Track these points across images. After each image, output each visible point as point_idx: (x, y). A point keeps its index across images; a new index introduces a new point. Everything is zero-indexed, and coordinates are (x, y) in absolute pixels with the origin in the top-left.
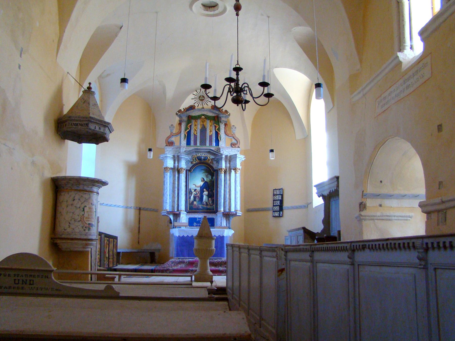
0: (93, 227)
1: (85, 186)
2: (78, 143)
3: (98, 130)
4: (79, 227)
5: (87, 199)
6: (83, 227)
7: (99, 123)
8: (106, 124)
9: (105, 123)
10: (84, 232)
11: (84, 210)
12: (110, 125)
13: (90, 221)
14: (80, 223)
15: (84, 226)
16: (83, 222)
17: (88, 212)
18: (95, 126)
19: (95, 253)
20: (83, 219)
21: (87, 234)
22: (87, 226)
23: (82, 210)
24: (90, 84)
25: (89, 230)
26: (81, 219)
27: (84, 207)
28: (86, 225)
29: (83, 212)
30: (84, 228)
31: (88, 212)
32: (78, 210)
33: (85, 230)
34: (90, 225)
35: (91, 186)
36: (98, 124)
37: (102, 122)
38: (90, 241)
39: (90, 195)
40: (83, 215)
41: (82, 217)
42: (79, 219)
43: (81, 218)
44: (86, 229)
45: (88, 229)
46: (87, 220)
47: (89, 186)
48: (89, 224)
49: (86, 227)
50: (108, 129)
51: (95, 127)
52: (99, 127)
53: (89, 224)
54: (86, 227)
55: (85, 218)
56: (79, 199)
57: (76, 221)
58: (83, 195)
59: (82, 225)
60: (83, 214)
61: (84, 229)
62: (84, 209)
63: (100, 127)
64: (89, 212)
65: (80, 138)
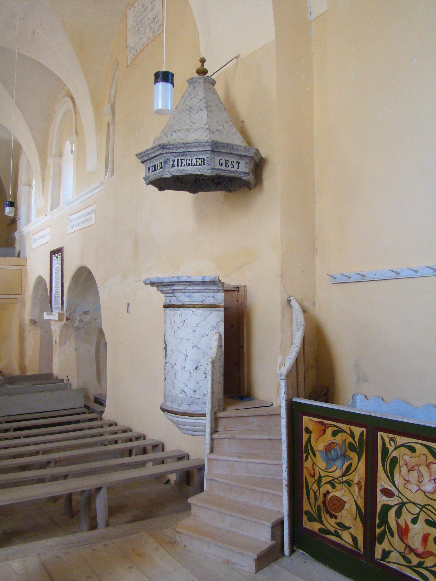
24: (203, 61)
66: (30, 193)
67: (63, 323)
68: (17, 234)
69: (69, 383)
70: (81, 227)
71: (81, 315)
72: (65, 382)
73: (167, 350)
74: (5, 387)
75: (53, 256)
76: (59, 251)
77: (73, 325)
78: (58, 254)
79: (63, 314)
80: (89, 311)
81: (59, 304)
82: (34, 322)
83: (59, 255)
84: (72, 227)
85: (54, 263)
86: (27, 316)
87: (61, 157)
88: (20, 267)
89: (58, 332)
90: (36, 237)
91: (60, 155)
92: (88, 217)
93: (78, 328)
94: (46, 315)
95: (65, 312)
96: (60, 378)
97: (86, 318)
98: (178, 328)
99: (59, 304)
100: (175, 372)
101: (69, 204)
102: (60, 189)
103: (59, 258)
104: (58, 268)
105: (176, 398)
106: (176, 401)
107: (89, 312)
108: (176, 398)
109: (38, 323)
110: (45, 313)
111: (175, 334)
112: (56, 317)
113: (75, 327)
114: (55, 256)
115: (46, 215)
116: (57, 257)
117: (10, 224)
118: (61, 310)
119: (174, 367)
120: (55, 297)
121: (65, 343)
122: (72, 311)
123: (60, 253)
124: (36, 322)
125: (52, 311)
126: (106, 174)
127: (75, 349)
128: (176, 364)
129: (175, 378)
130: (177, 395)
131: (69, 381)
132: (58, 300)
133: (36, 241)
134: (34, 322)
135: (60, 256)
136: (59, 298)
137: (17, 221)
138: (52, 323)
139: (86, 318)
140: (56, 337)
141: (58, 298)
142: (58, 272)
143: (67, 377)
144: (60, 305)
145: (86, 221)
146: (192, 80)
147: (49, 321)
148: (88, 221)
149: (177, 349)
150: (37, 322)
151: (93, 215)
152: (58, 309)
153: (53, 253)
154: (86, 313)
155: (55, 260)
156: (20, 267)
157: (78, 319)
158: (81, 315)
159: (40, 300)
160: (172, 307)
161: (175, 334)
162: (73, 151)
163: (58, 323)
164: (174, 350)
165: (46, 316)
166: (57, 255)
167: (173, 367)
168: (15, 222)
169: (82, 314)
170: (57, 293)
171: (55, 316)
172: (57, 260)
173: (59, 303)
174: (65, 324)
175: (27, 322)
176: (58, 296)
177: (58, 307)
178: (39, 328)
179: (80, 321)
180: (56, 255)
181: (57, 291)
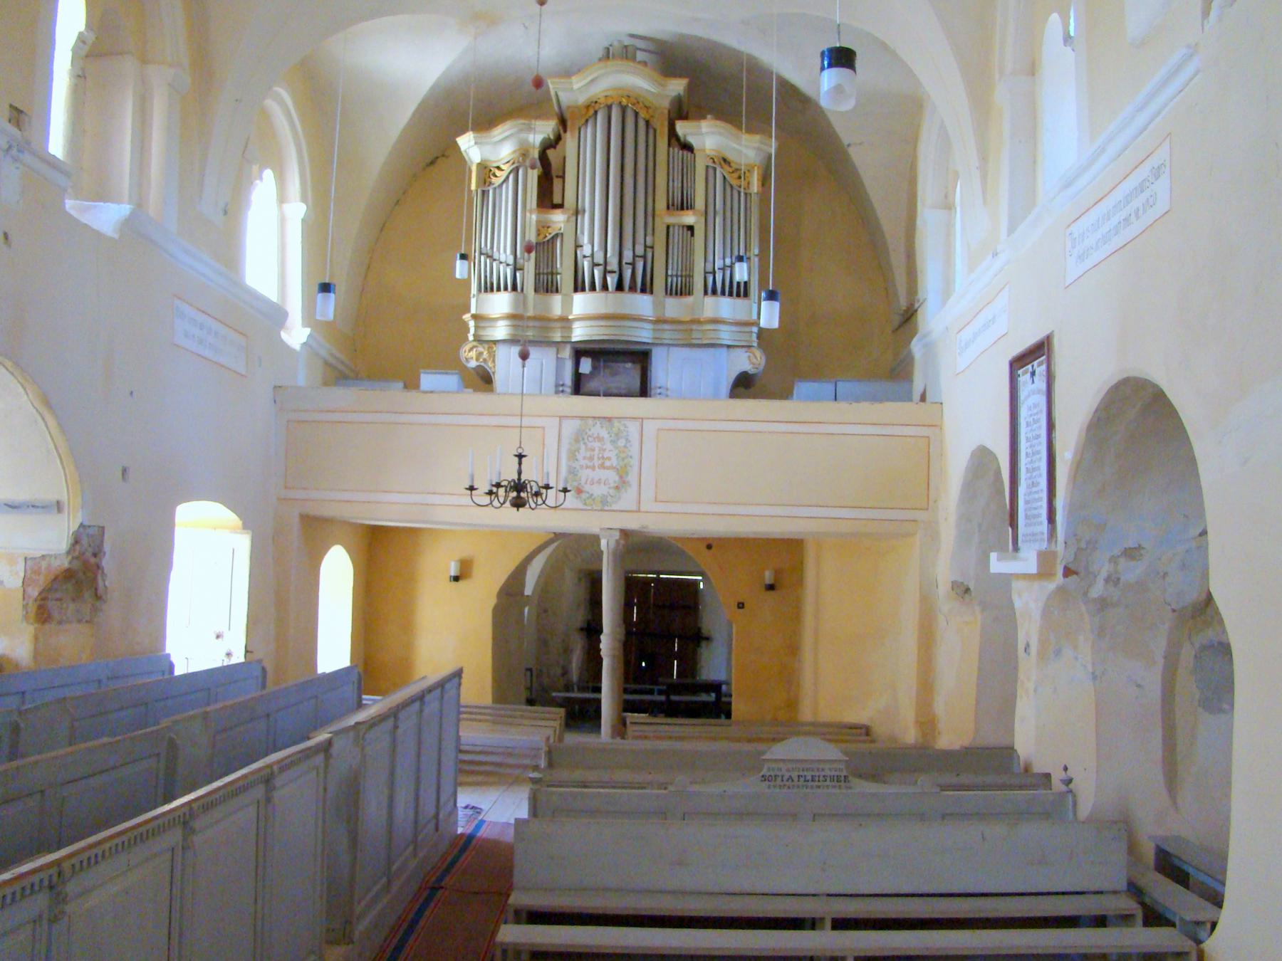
66: (949, 226)
67: (1051, 586)
68: (916, 347)
69: (1071, 791)
70: (1117, 241)
71: (1113, 560)
72: (1057, 786)
74: (850, 788)
75: (1020, 372)
76: (1040, 350)
77: (1085, 594)
78: (1035, 363)
79: (1054, 554)
80: (1140, 548)
81: (1041, 523)
82: (962, 590)
83: (1040, 365)
84: (1081, 258)
85: (1023, 394)
86: (944, 572)
87: (1033, 75)
88: (925, 431)
89: (1036, 615)
90: (967, 334)
91: (1032, 69)
92: (1137, 202)
93: (1103, 604)
94: (999, 559)
95: (1060, 547)
96: (1038, 768)
97: (1132, 572)
99: (1041, 523)
101: (1068, 185)
102: (1034, 170)
103: (1040, 376)
104: (1035, 406)
107: (1142, 552)
109: (973, 594)
110: (993, 556)
112: (1033, 569)
113: (1094, 600)
114: (1025, 373)
115: (995, 254)
116: (1033, 374)
117: (900, 326)
118: (1046, 543)
120: (1027, 502)
121: (1058, 652)
122: (1083, 545)
123: (1044, 357)
124: (967, 590)
125: (1016, 548)
126: (1206, 13)
127: (1093, 673)
131: (1071, 786)
132: (1035, 512)
133: (967, 345)
134: (964, 589)
135: (1044, 367)
136: (1039, 504)
137: (916, 311)
138: (1016, 585)
139: (1132, 572)
140: (1029, 630)
141: (1035, 505)
142: (1035, 421)
143: (1066, 769)
144: (1044, 527)
145: (1133, 216)
147: (1007, 579)
148: (1141, 212)
150: (972, 588)
151: (1164, 182)
152: (1035, 541)
153: (1020, 361)
154: (1132, 553)
155: (1025, 383)
156: (925, 431)
157: (1104, 574)
158: (1113, 560)
159: (980, 526)
162: (1072, 34)
163: (1036, 585)
165: (998, 565)
166: (1033, 366)
168: (912, 315)
169: (1118, 556)
170: (1034, 489)
171: (1027, 561)
172: (1033, 382)
173: (1040, 519)
174: (1060, 590)
175: (943, 588)
176: (1036, 496)
177: (1033, 534)
178: (978, 609)
179: (1112, 580)
180: (1029, 367)
181: (1034, 480)
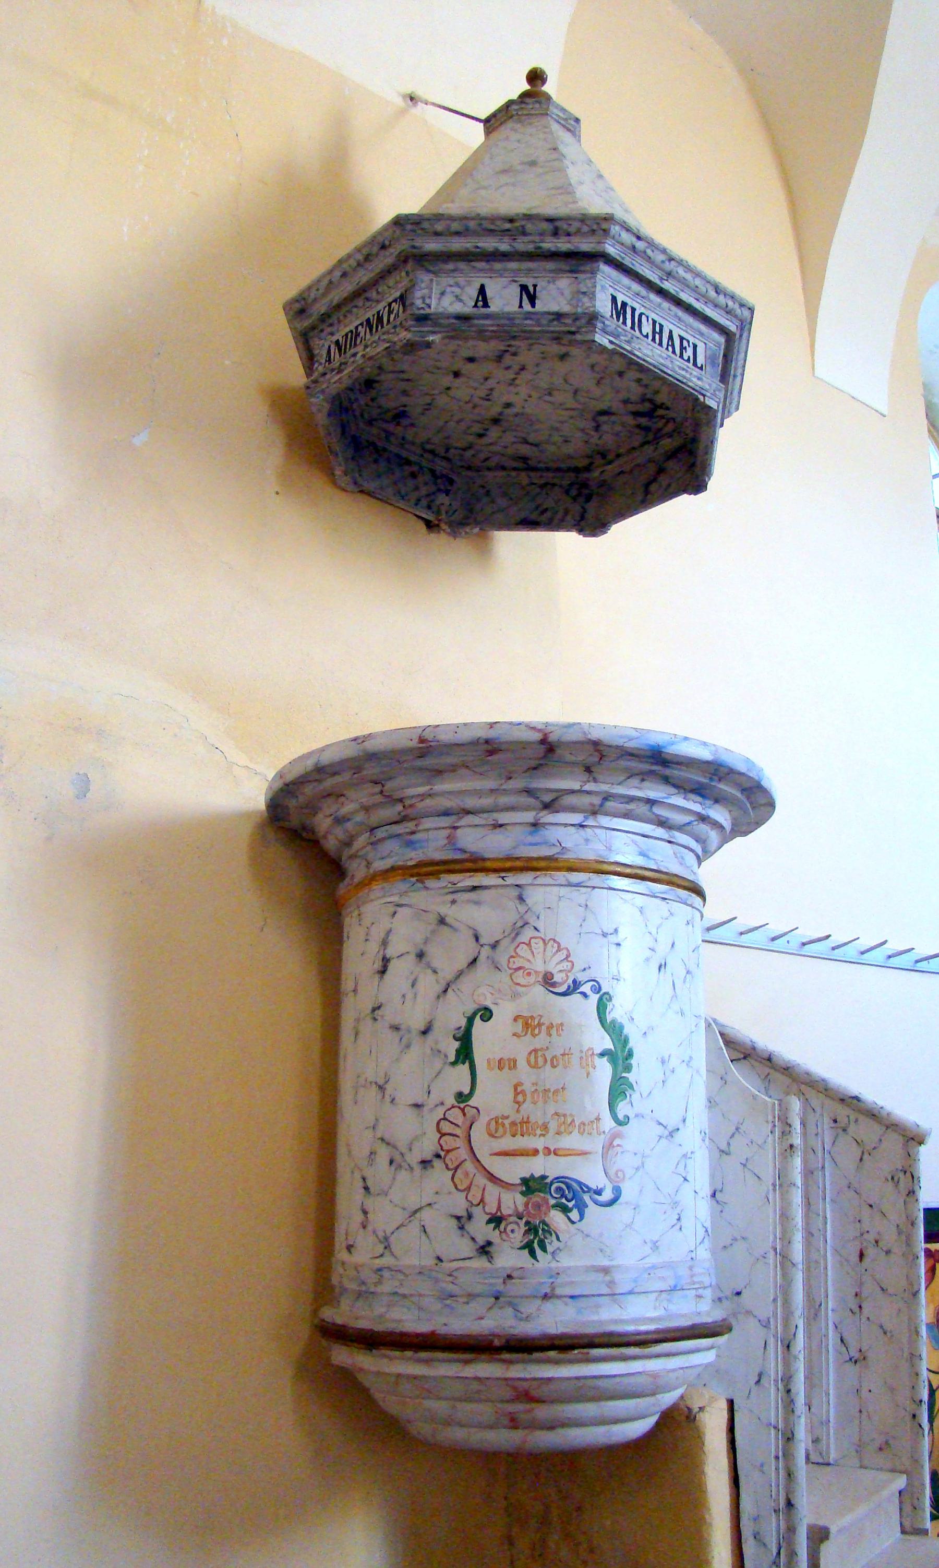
0: (592, 1210)
1: (470, 819)
2: (581, 531)
3: (513, 307)
4: (426, 1216)
5: (494, 946)
6: (462, 1221)
7: (504, 247)
8: (575, 240)
9: (556, 233)
10: (481, 1263)
11: (465, 1053)
12: (615, 229)
13: (536, 1152)
14: (439, 1175)
15: (477, 1211)
16: (469, 1166)
17: (513, 1064)
18: (473, 292)
19: (773, 1442)
20: (459, 1143)
21: (515, 1287)
22: (512, 1201)
23: (453, 1047)
25: (529, 1247)
26: (448, 1142)
27: (471, 1020)
28: (493, 1191)
29: (464, 1068)
30: (481, 1229)
31: (513, 1064)
32: (418, 1049)
33: (485, 1250)
34: (537, 1198)
35: (529, 817)
36: (498, 266)
37: (524, 233)
38: (537, 1355)
39: (521, 899)
40: (460, 1097)
41: (456, 1115)
42: (428, 1146)
43: (446, 1126)
44: (494, 1236)
45: (518, 1235)
46: (508, 1143)
47: (504, 818)
48: (525, 1181)
49: (496, 1220)
50: (614, 273)
51: (482, 290)
52: (524, 288)
53: (531, 1185)
54: (496, 1220)
55: (478, 1134)
56: (421, 955)
57: (400, 1167)
58: (451, 913)
59: (459, 1204)
60: (466, 1091)
61: (481, 1241)
62: (465, 1041)
63: (524, 281)
64: (522, 1063)
65: (589, 498)
73: (633, 1061)
98: (688, 972)
100: (685, 1156)
105: (691, 1268)
106: (695, 1279)
108: (691, 1268)
111: (675, 996)
119: (678, 1137)
128: (684, 1121)
129: (685, 1179)
130: (693, 1255)
146: (572, 122)
149: (687, 1059)
160: (668, 883)
161: (675, 996)
164: (674, 1062)
167: (671, 1134)
